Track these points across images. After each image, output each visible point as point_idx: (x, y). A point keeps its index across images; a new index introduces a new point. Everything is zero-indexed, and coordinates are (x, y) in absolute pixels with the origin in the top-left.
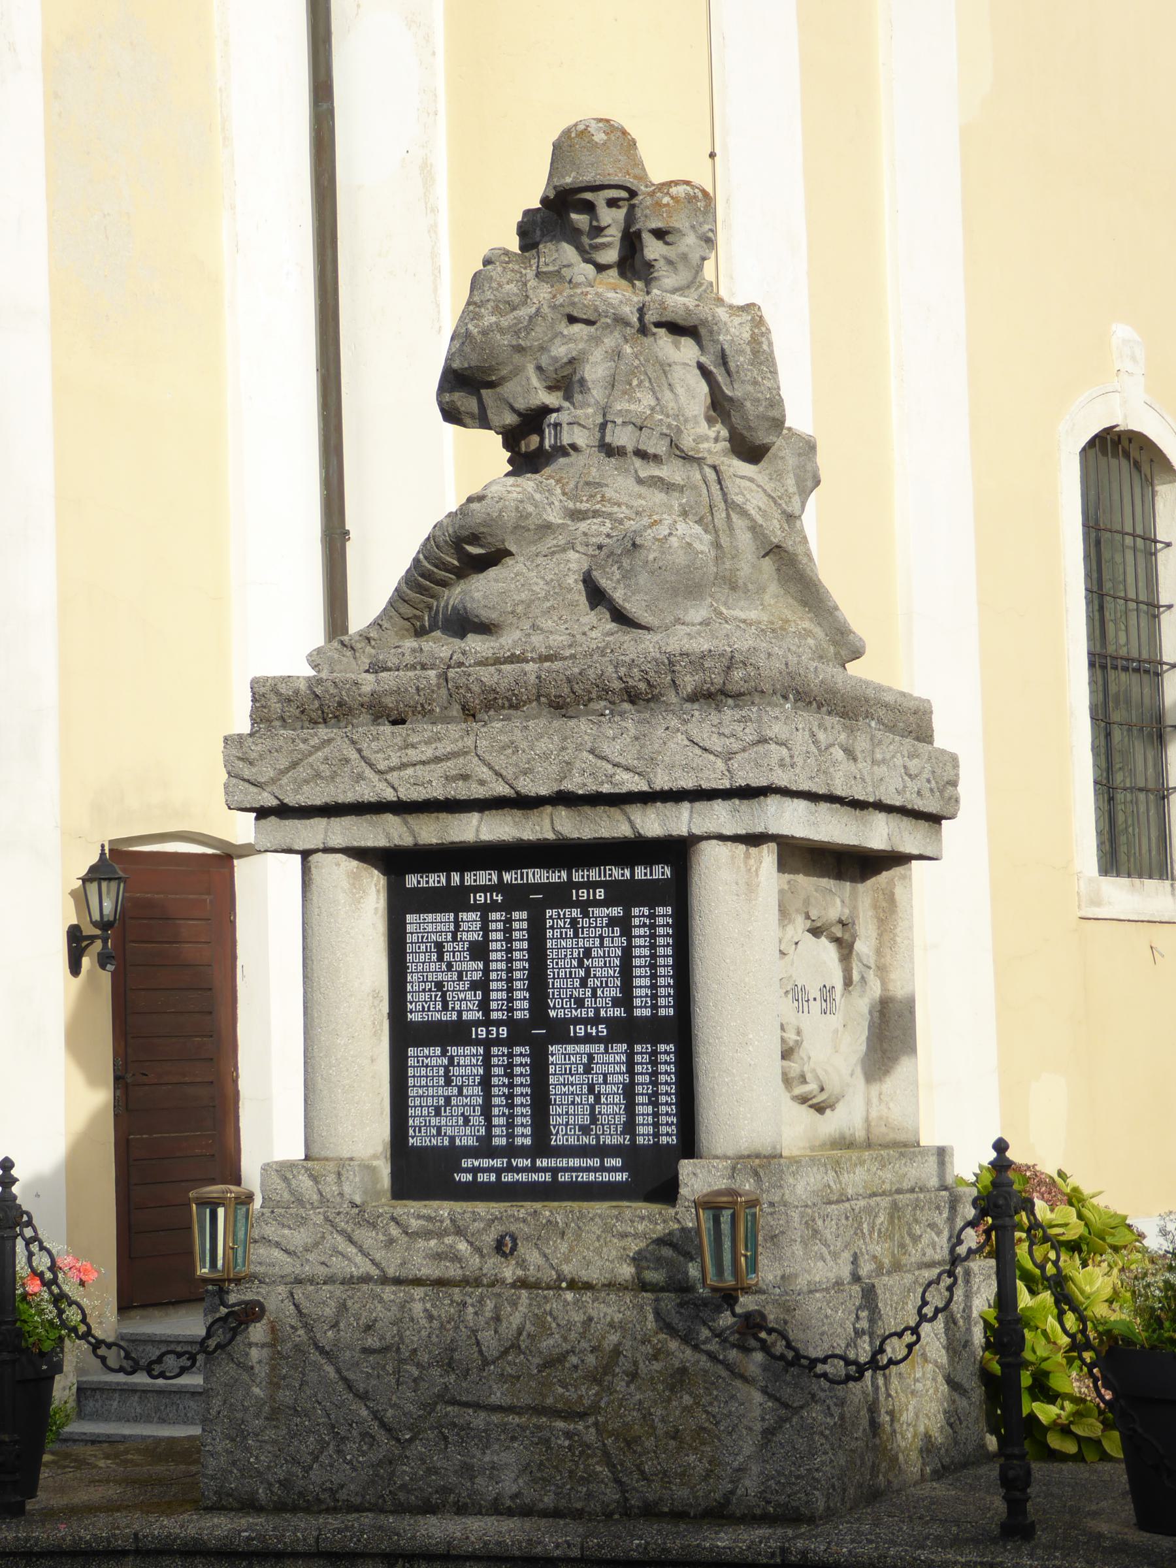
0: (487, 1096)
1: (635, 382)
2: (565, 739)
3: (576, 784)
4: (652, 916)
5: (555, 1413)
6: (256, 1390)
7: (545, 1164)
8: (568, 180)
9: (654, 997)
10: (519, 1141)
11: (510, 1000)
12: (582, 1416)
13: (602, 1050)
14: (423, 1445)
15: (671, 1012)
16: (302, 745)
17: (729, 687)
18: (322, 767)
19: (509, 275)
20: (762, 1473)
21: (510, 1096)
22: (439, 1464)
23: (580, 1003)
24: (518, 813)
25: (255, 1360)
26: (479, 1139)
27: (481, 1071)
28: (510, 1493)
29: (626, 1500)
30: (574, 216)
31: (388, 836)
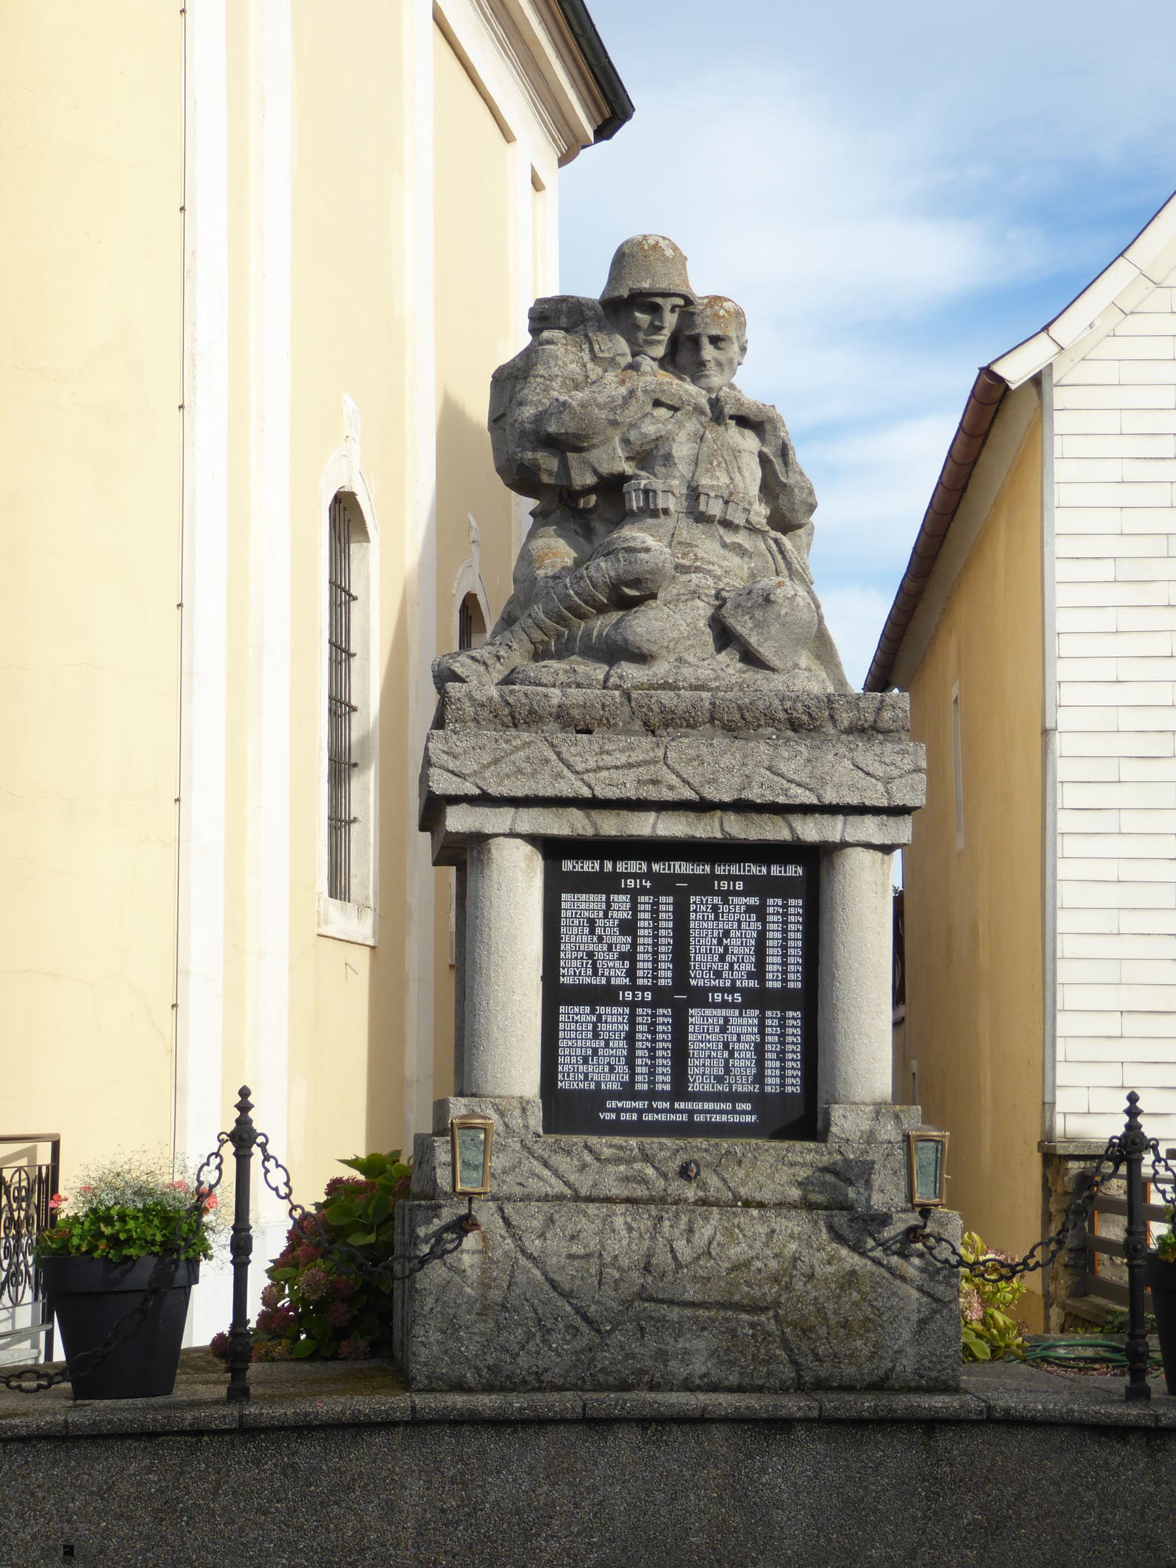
0: (632, 1049)
1: (715, 463)
2: (746, 756)
3: (755, 794)
4: (785, 906)
5: (740, 1307)
6: (468, 1290)
7: (682, 1106)
8: (647, 286)
9: (785, 972)
10: (659, 1087)
11: (655, 969)
12: (764, 1309)
13: (737, 1014)
14: (622, 1335)
15: (799, 985)
16: (504, 745)
17: (880, 725)
18: (524, 765)
19: (571, 356)
20: (918, 1354)
21: (653, 1050)
22: (636, 1351)
23: (718, 974)
24: (692, 815)
25: (467, 1265)
26: (623, 1084)
28: (699, 1373)
29: (800, 1377)
30: (638, 315)
31: (572, 827)
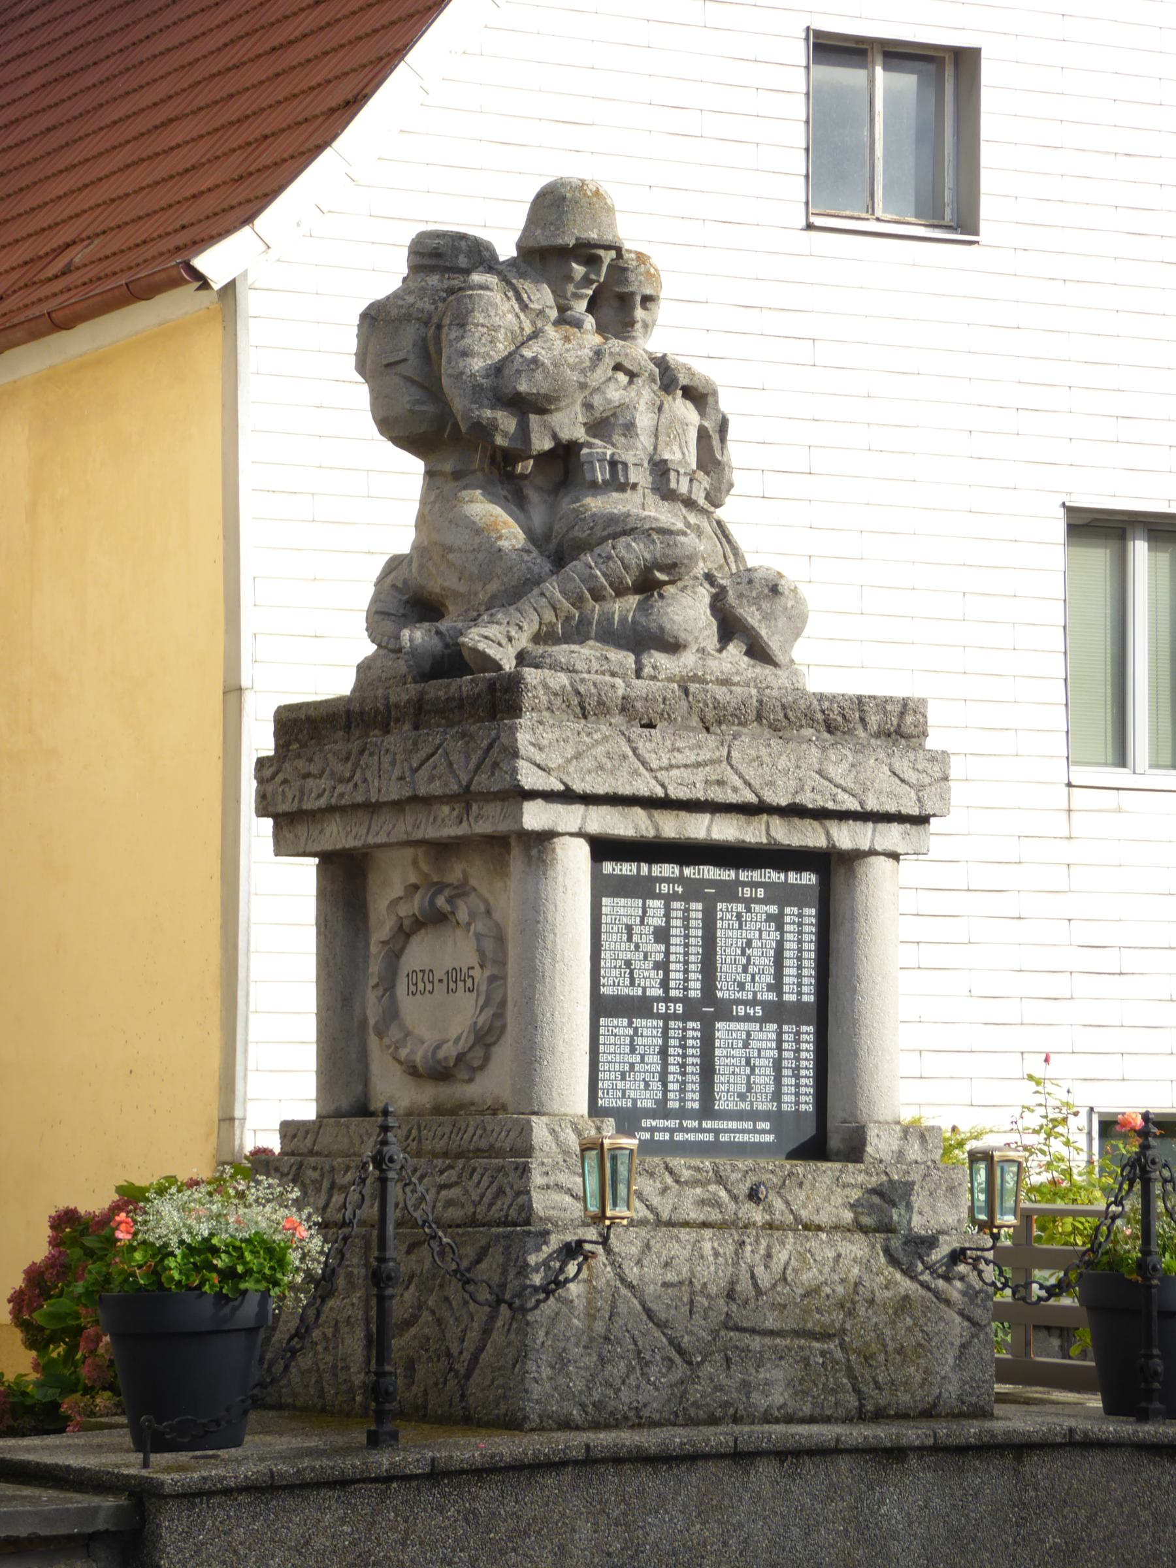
0: (665, 1064)
3: (808, 800)
4: (800, 916)
6: (575, 1321)
7: (709, 1126)
8: (596, 236)
9: (800, 985)
10: (689, 1105)
11: (686, 980)
13: (758, 1028)
15: (812, 998)
18: (604, 760)
21: (683, 1065)
22: (724, 1382)
24: (742, 818)
26: (657, 1102)
27: (660, 1042)
30: (574, 265)
